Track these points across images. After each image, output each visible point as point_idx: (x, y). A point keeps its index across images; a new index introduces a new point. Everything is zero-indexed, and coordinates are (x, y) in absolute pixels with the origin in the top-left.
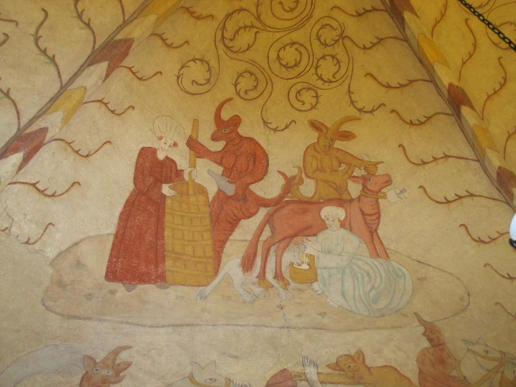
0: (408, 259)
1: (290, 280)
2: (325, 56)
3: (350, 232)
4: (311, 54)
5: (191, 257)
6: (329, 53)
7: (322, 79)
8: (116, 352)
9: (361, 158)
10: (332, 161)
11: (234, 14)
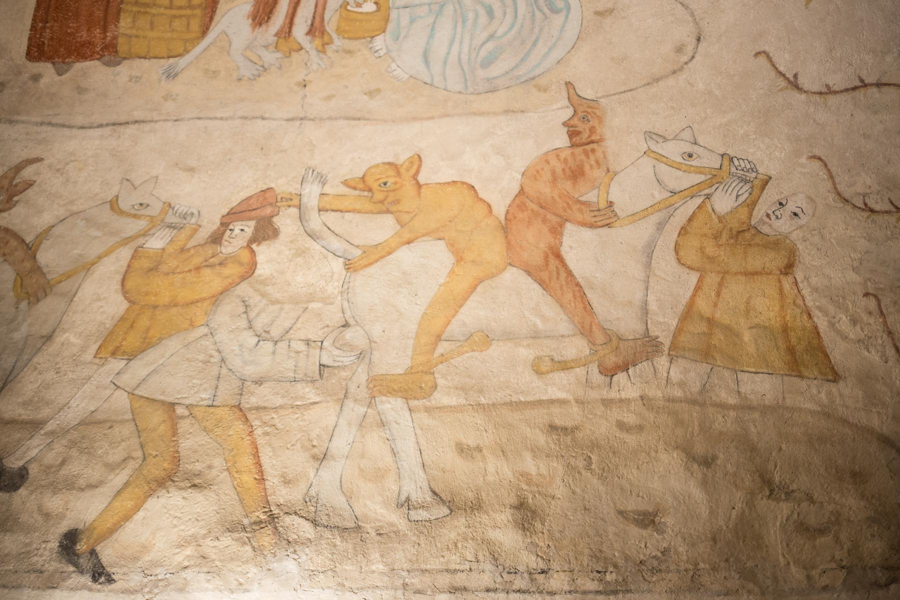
1: (334, 36)
5: (166, 8)
8: (19, 168)
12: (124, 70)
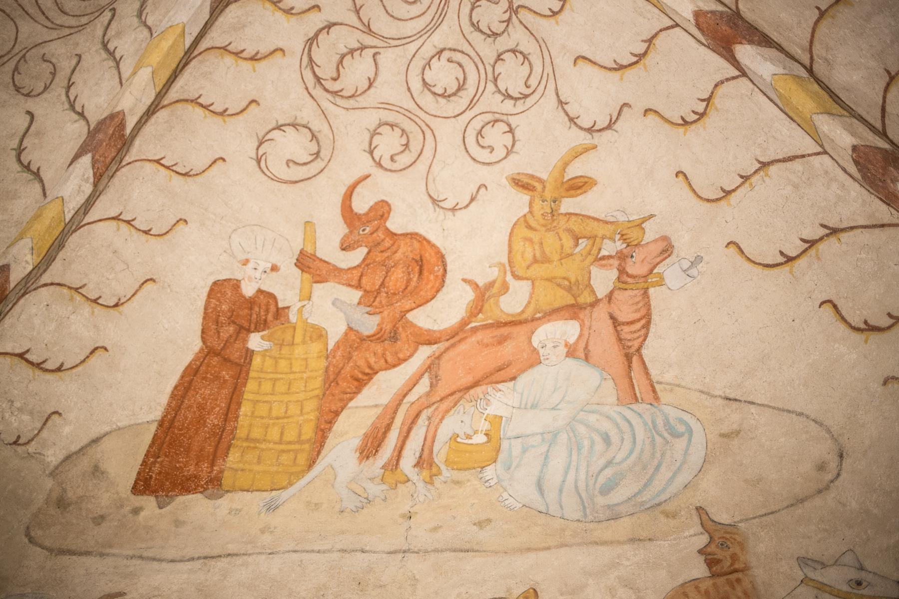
0: (704, 396)
1: (443, 467)
2: (502, 54)
3: (584, 363)
4: (477, 59)
5: (275, 443)
6: (506, 48)
7: (510, 97)
9: (612, 219)
10: (561, 240)
11: (320, 37)
12: (225, 503)
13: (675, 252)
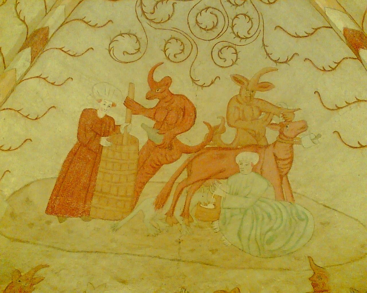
1: (194, 218)
8: (36, 269)
12: (92, 224)
13: (308, 129)
